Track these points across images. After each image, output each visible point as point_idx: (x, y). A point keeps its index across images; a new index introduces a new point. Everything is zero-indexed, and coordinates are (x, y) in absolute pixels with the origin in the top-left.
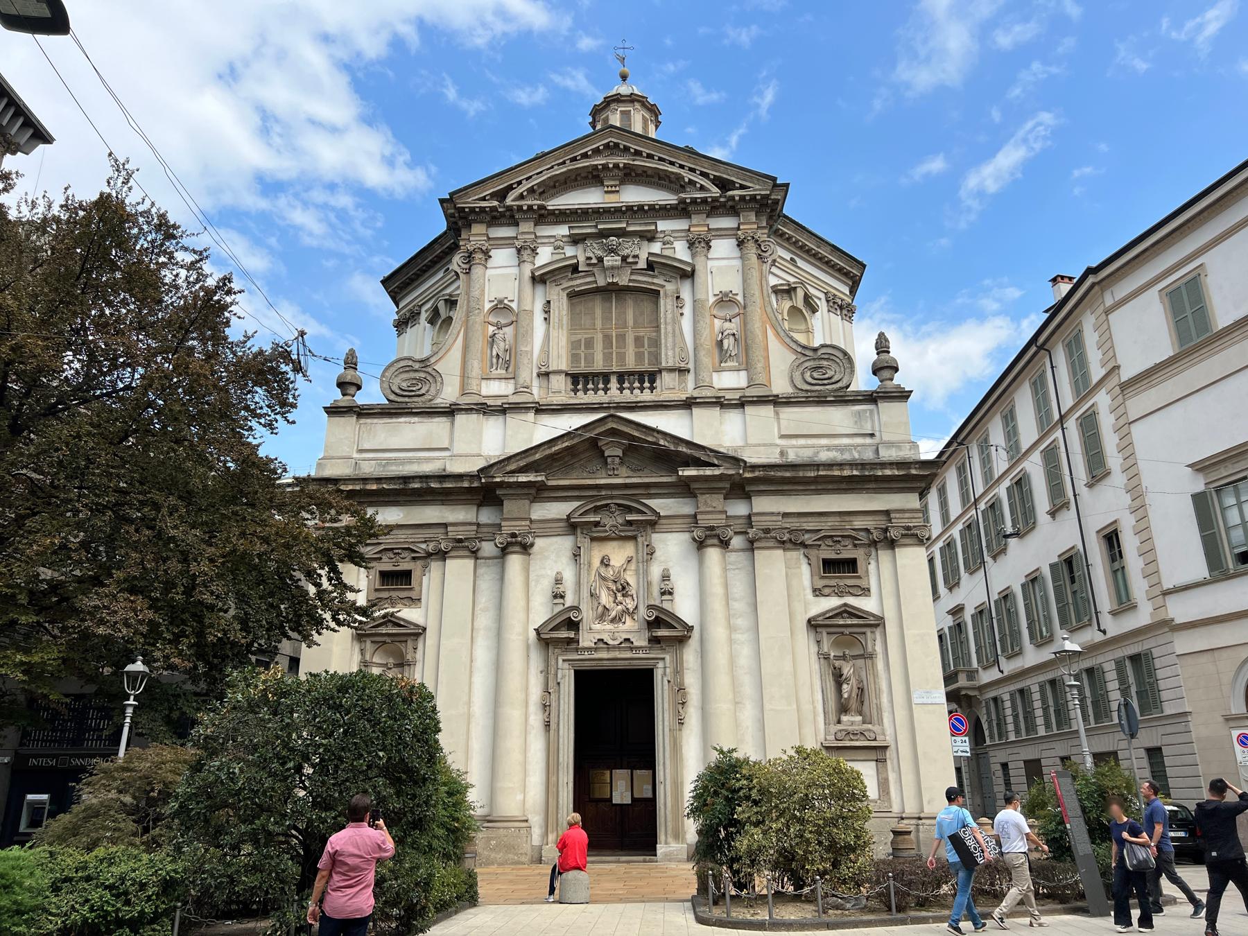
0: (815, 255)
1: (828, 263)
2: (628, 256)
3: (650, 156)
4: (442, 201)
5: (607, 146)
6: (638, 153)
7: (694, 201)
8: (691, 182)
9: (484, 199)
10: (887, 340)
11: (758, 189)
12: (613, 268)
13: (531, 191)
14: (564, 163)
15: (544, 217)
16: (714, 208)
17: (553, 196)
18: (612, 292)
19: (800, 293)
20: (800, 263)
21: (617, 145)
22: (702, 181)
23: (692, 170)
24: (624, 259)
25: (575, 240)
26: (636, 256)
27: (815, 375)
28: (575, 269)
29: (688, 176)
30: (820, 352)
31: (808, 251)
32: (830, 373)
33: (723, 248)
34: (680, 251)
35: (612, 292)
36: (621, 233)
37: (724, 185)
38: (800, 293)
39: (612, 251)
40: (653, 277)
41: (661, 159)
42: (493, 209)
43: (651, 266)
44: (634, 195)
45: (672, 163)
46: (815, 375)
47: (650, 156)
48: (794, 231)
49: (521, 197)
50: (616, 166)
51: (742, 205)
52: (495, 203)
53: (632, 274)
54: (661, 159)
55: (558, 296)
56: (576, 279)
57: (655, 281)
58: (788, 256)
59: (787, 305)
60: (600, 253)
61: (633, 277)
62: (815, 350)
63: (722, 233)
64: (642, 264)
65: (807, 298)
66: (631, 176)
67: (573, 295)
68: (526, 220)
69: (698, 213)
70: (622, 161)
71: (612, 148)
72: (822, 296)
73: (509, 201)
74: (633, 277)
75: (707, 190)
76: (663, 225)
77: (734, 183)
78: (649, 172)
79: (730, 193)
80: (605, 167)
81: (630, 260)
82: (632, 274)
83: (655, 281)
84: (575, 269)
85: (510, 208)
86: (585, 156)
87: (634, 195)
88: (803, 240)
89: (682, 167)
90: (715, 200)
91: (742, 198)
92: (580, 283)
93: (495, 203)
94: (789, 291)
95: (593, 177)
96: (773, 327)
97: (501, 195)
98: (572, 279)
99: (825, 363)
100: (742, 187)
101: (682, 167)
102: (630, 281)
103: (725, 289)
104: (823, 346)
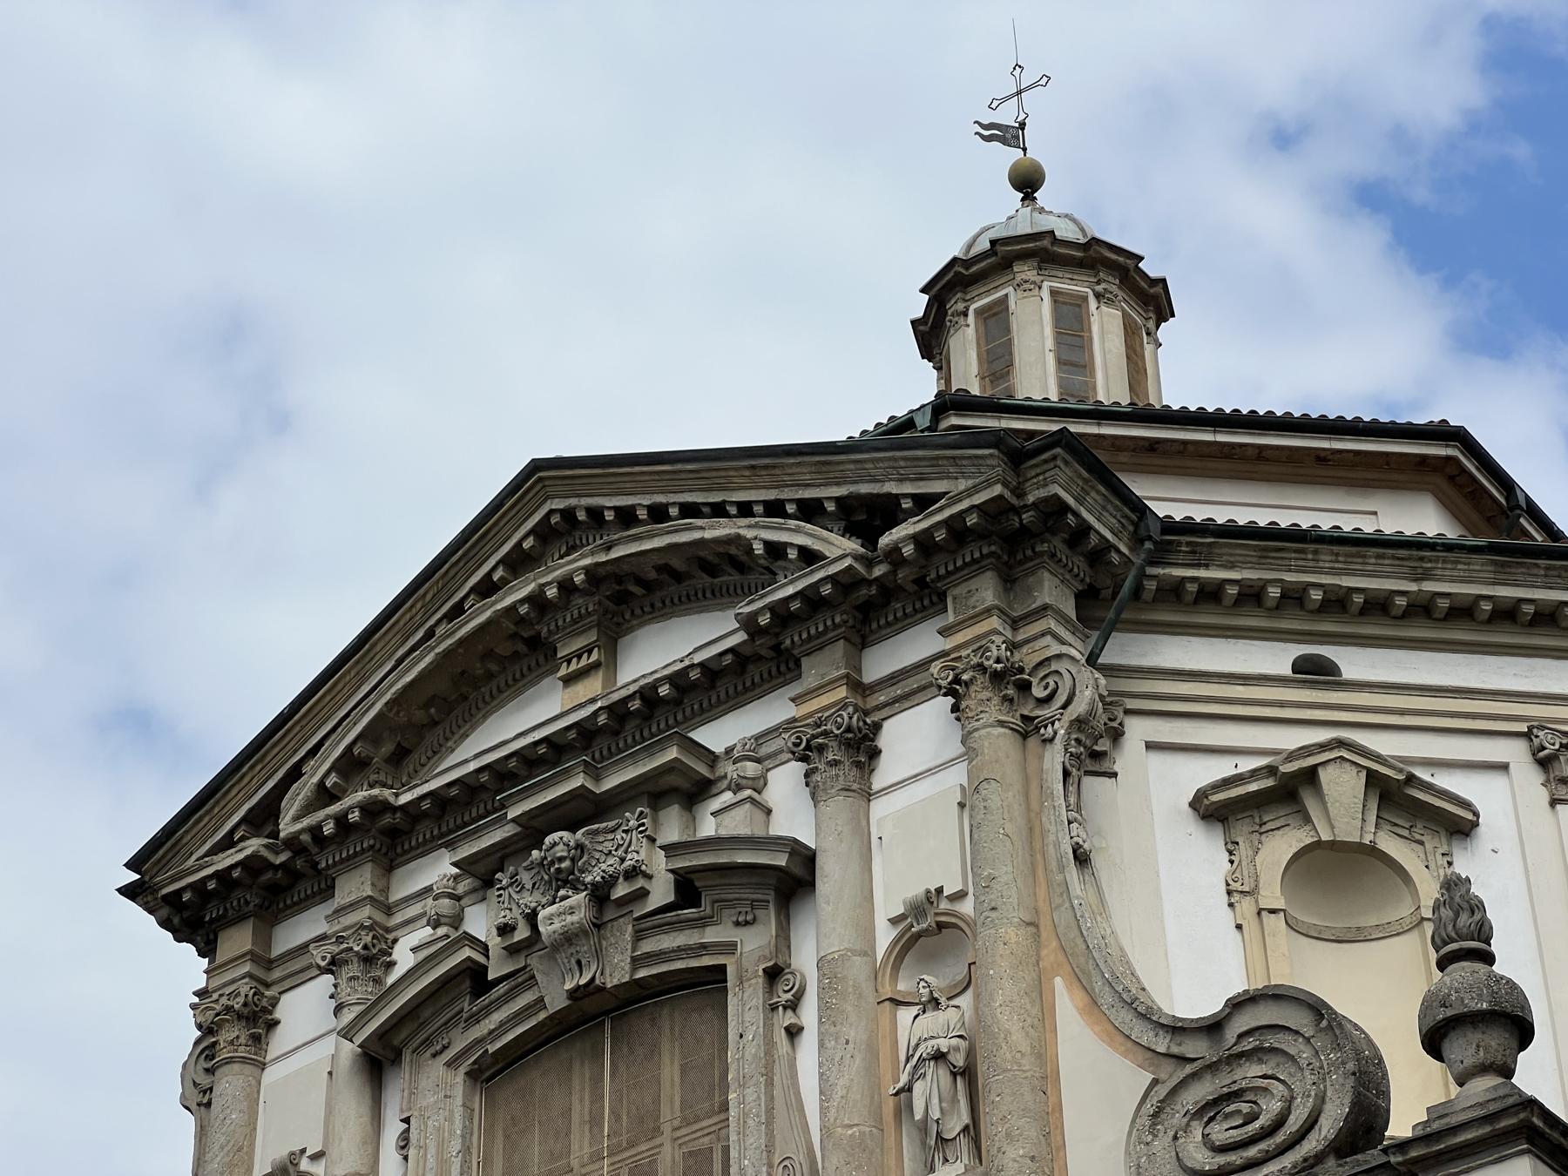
0: (1422, 609)
1: (1507, 614)
2: (610, 881)
3: (658, 514)
4: (128, 891)
5: (544, 533)
6: (626, 517)
7: (780, 612)
8: (776, 550)
9: (228, 843)
10: (1476, 907)
11: (965, 491)
12: (569, 938)
13: (351, 766)
14: (430, 634)
15: (395, 838)
16: (868, 608)
17: (438, 752)
18: (595, 1017)
19: (1343, 788)
20: (1354, 663)
21: (568, 514)
22: (798, 535)
23: (775, 509)
24: (600, 895)
25: (483, 874)
26: (633, 873)
27: (1221, 1132)
28: (474, 978)
29: (758, 533)
30: (1231, 1034)
31: (1378, 606)
32: (1270, 1108)
33: (916, 738)
34: (791, 807)
35: (595, 1017)
36: (584, 811)
37: (866, 518)
38: (1343, 788)
39: (562, 880)
40: (701, 923)
41: (690, 510)
42: (252, 865)
43: (687, 889)
44: (659, 651)
45: (719, 510)
46: (1221, 1132)
47: (658, 514)
48: (1261, 561)
49: (325, 795)
50: (566, 586)
51: (939, 565)
52: (254, 845)
53: (639, 936)
54: (690, 510)
55: (436, 1092)
56: (487, 1011)
57: (711, 935)
58: (1277, 658)
59: (1282, 845)
60: (529, 900)
61: (648, 946)
62: (1213, 1027)
63: (908, 688)
64: (661, 892)
65: (1395, 795)
66: (629, 598)
67: (490, 1073)
68: (350, 864)
69: (817, 645)
70: (576, 565)
71: (560, 532)
72: (1515, 753)
73: (287, 827)
74: (648, 946)
75: (809, 557)
76: (717, 735)
77: (896, 499)
78: (677, 563)
79: (885, 540)
80: (536, 600)
81: (621, 890)
82: (639, 936)
83: (711, 935)
84: (474, 978)
85: (292, 843)
86: (487, 588)
87: (659, 651)
88: (1322, 578)
89: (745, 509)
90: (846, 583)
91: (923, 541)
92: (498, 1024)
93: (254, 845)
94: (1289, 790)
95: (518, 652)
96: (1080, 980)
97: (264, 817)
98: (475, 1019)
99: (1254, 1070)
100: (923, 503)
101: (745, 509)
102: (637, 962)
103: (916, 890)
104: (1237, 1004)
